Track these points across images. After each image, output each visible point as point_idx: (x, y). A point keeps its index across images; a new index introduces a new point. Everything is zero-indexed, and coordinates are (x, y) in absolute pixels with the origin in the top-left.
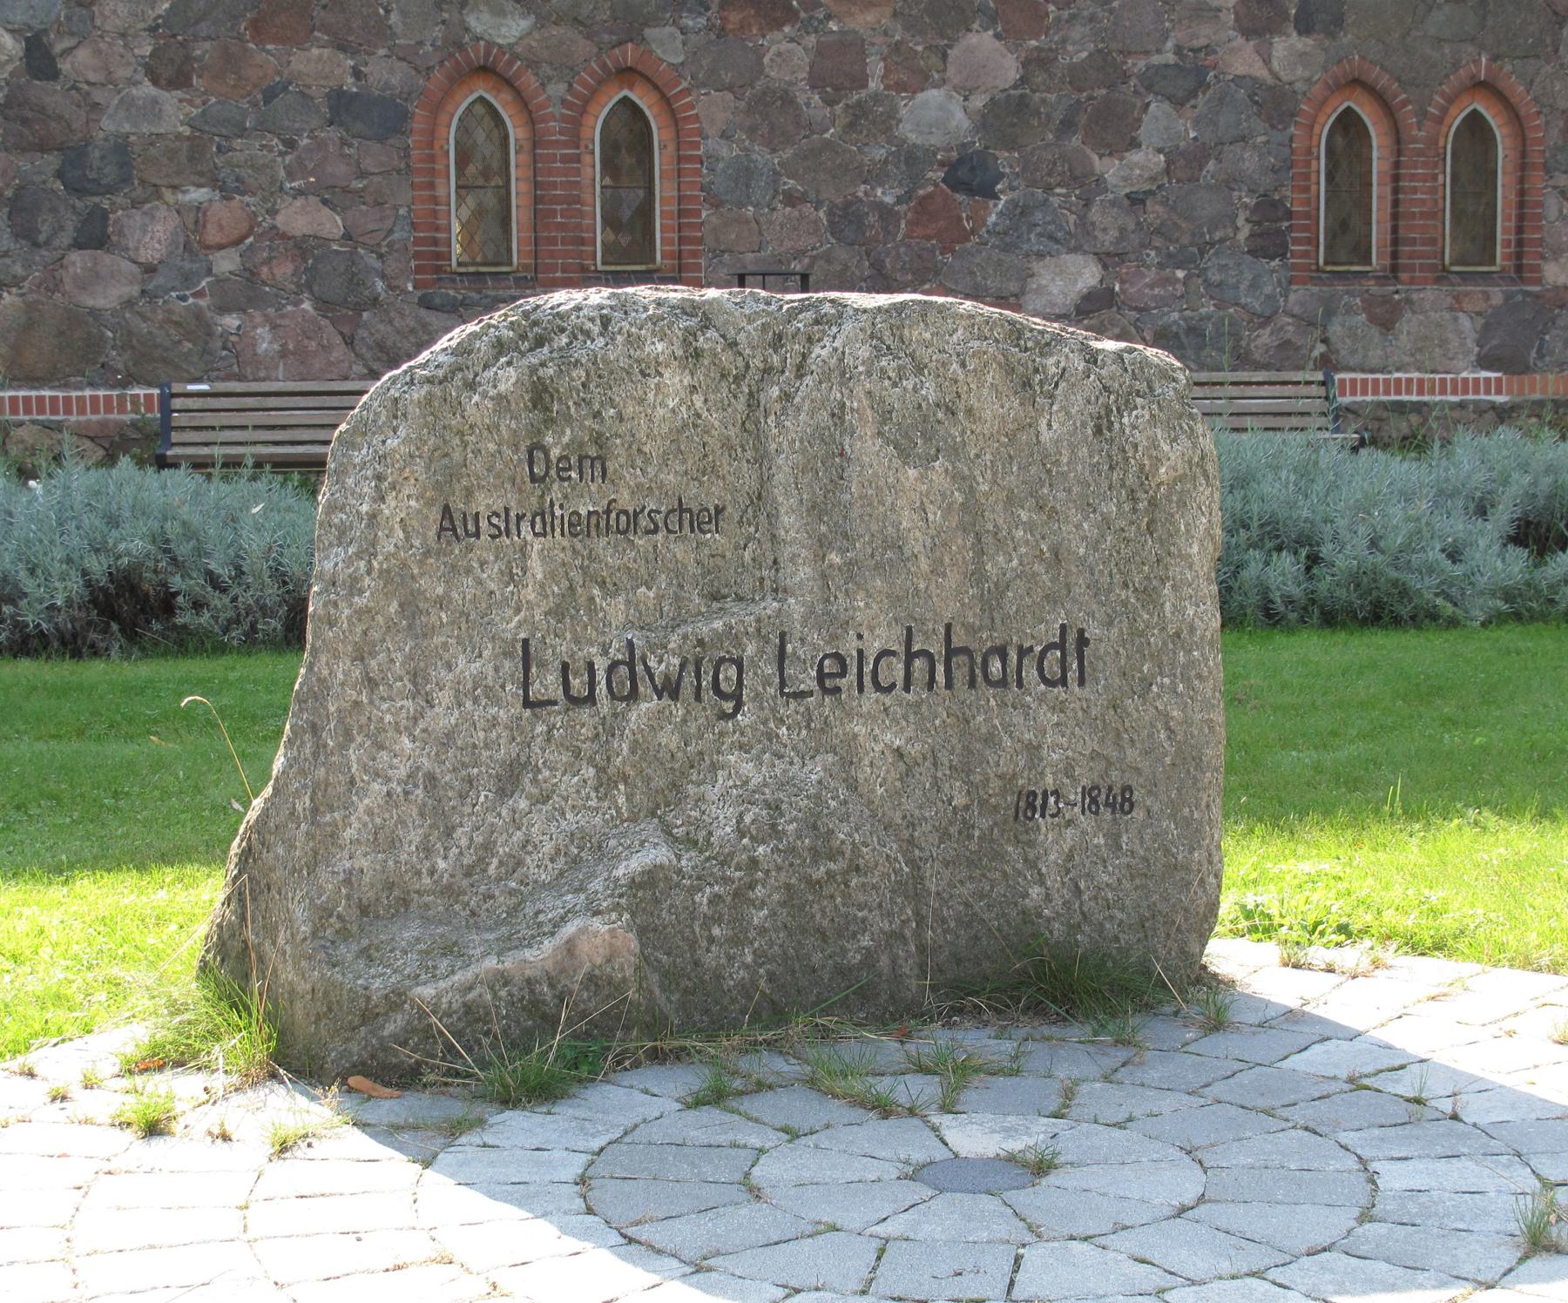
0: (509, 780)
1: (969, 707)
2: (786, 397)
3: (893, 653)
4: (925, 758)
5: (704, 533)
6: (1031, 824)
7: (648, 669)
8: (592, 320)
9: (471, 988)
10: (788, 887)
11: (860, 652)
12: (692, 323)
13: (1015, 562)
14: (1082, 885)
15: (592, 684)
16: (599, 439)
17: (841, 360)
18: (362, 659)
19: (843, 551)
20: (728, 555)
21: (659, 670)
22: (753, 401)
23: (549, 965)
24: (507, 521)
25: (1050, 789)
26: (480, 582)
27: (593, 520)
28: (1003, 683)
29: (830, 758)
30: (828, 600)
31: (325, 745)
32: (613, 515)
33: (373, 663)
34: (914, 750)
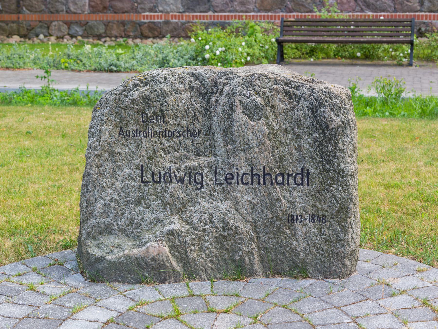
0: (138, 202)
1: (271, 190)
2: (217, 101)
3: (248, 174)
4: (258, 204)
5: (195, 137)
6: (293, 224)
7: (175, 175)
8: (162, 78)
9: (120, 258)
10: (216, 237)
11: (238, 173)
12: (192, 79)
13: (287, 149)
14: (310, 242)
15: (160, 178)
16: (162, 111)
17: (232, 91)
18: (98, 168)
19: (232, 145)
20: (202, 143)
21: (178, 175)
22: (208, 102)
23: (142, 254)
24: (137, 133)
25: (299, 214)
26: (130, 149)
27: (161, 133)
28: (282, 184)
29: (230, 202)
30: (228, 158)
31: (89, 190)
32: (167, 132)
33: (101, 169)
34: (255, 201)
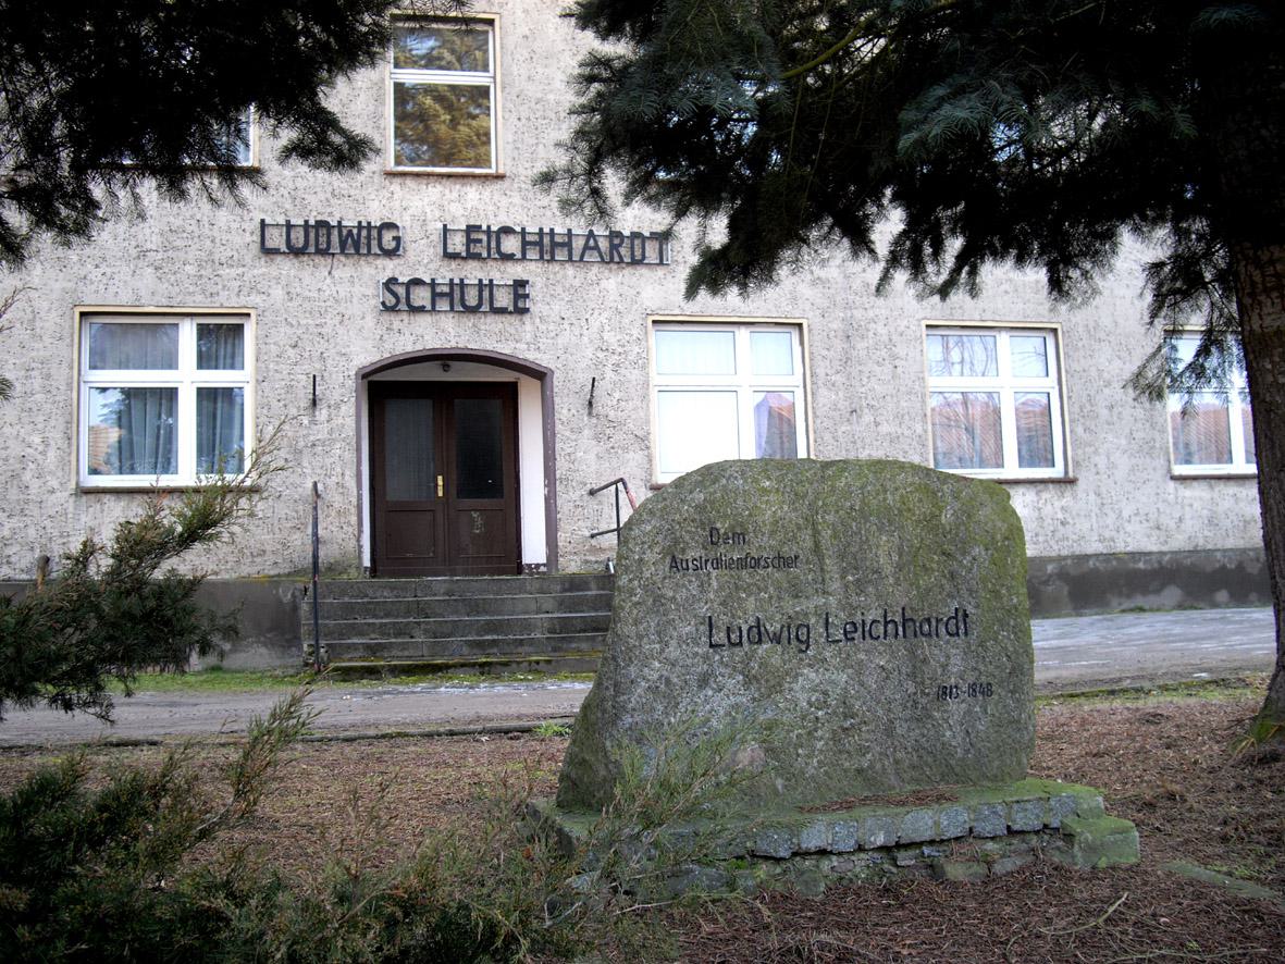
0: (703, 682)
15: (741, 637)
19: (853, 575)
29: (850, 671)
